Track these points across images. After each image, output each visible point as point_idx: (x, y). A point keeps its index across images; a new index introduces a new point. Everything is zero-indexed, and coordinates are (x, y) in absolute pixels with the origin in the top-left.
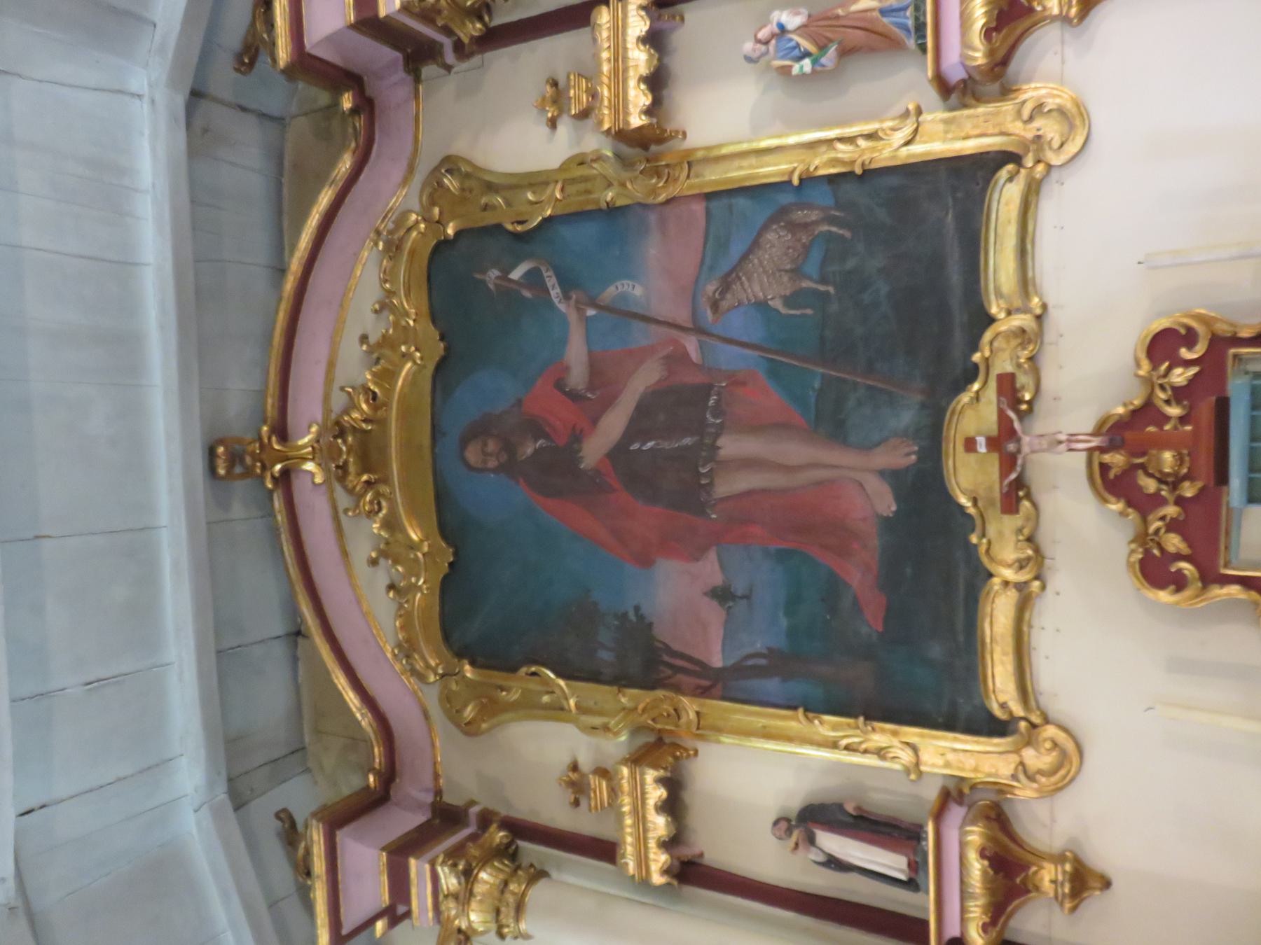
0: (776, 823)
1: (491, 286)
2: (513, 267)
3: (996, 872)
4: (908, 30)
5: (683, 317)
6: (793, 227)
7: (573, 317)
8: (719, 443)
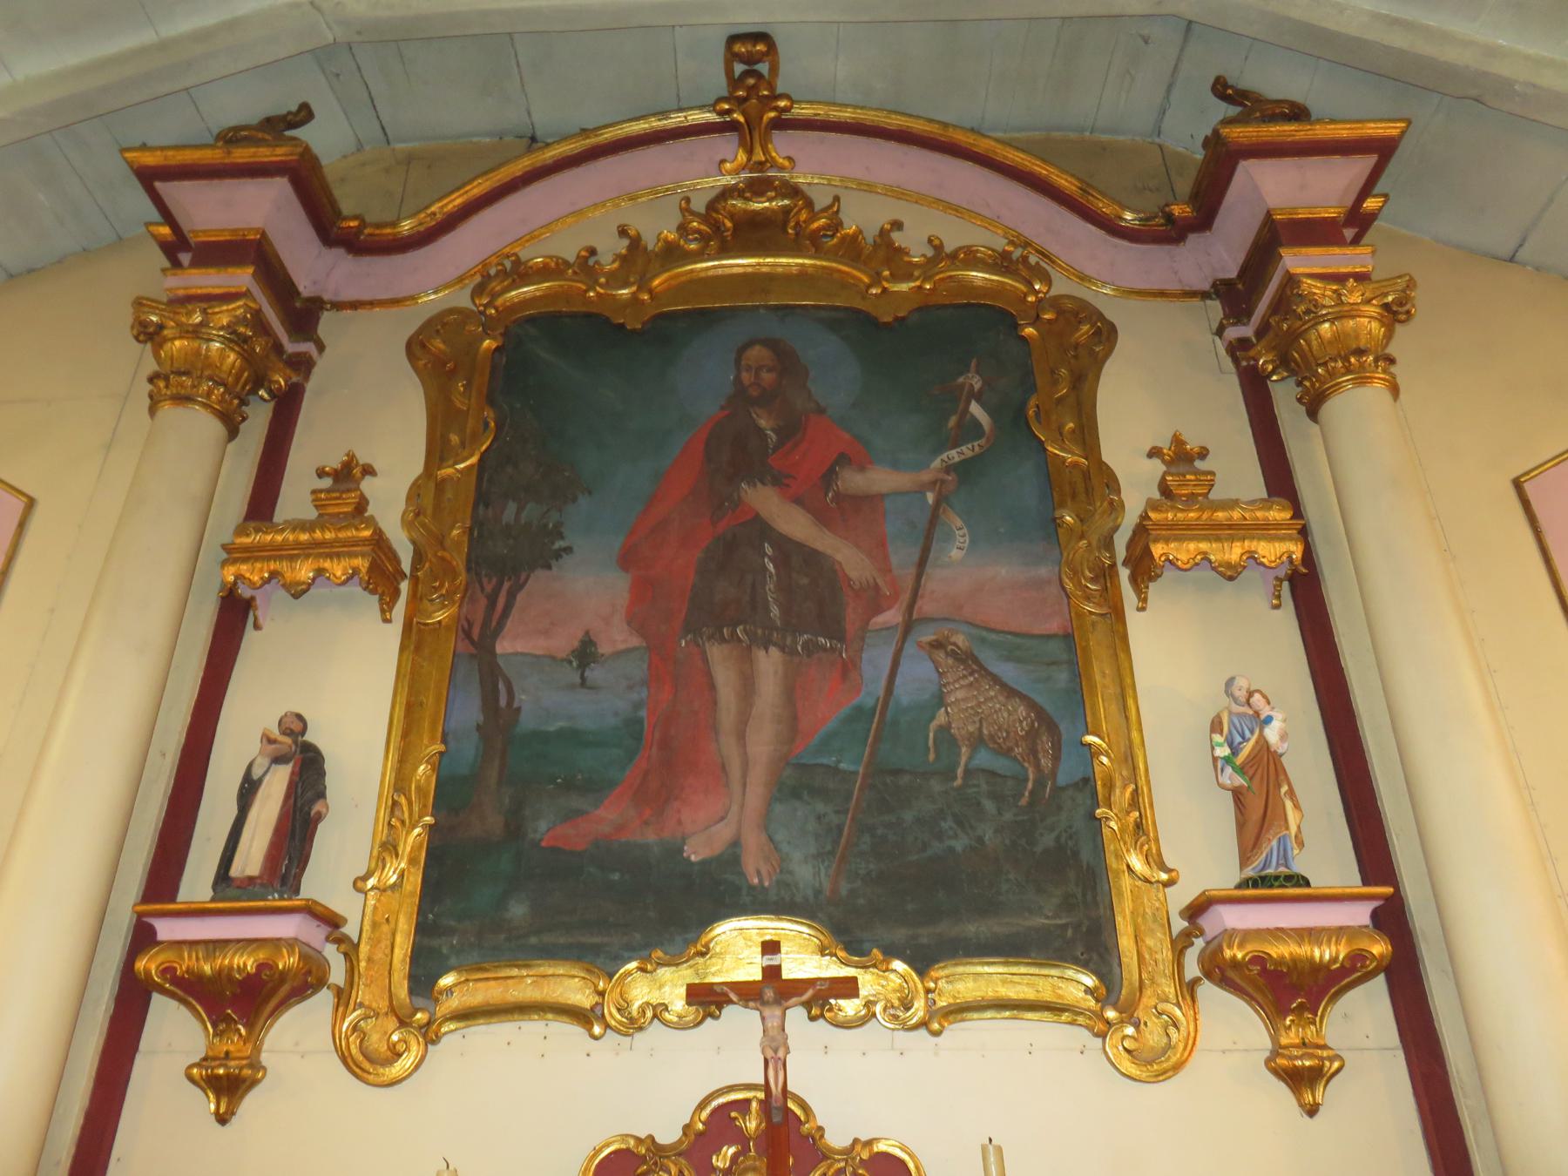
0: (300, 717)
1: (961, 380)
3: (241, 983)
4: (1264, 868)
5: (926, 606)
6: (1032, 735)
7: (926, 476)
8: (773, 651)
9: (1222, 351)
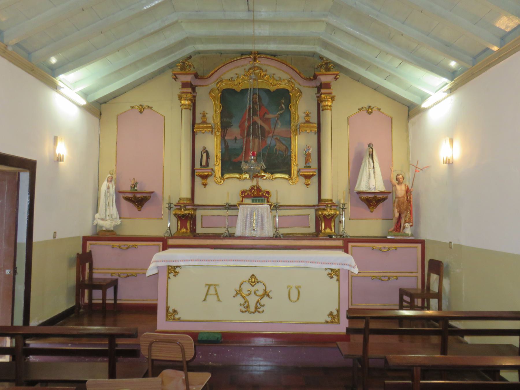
0: (205, 147)
1: (281, 101)
2: (284, 105)
5: (275, 133)
6: (285, 150)
7: (276, 115)
8: (257, 139)
9: (316, 97)
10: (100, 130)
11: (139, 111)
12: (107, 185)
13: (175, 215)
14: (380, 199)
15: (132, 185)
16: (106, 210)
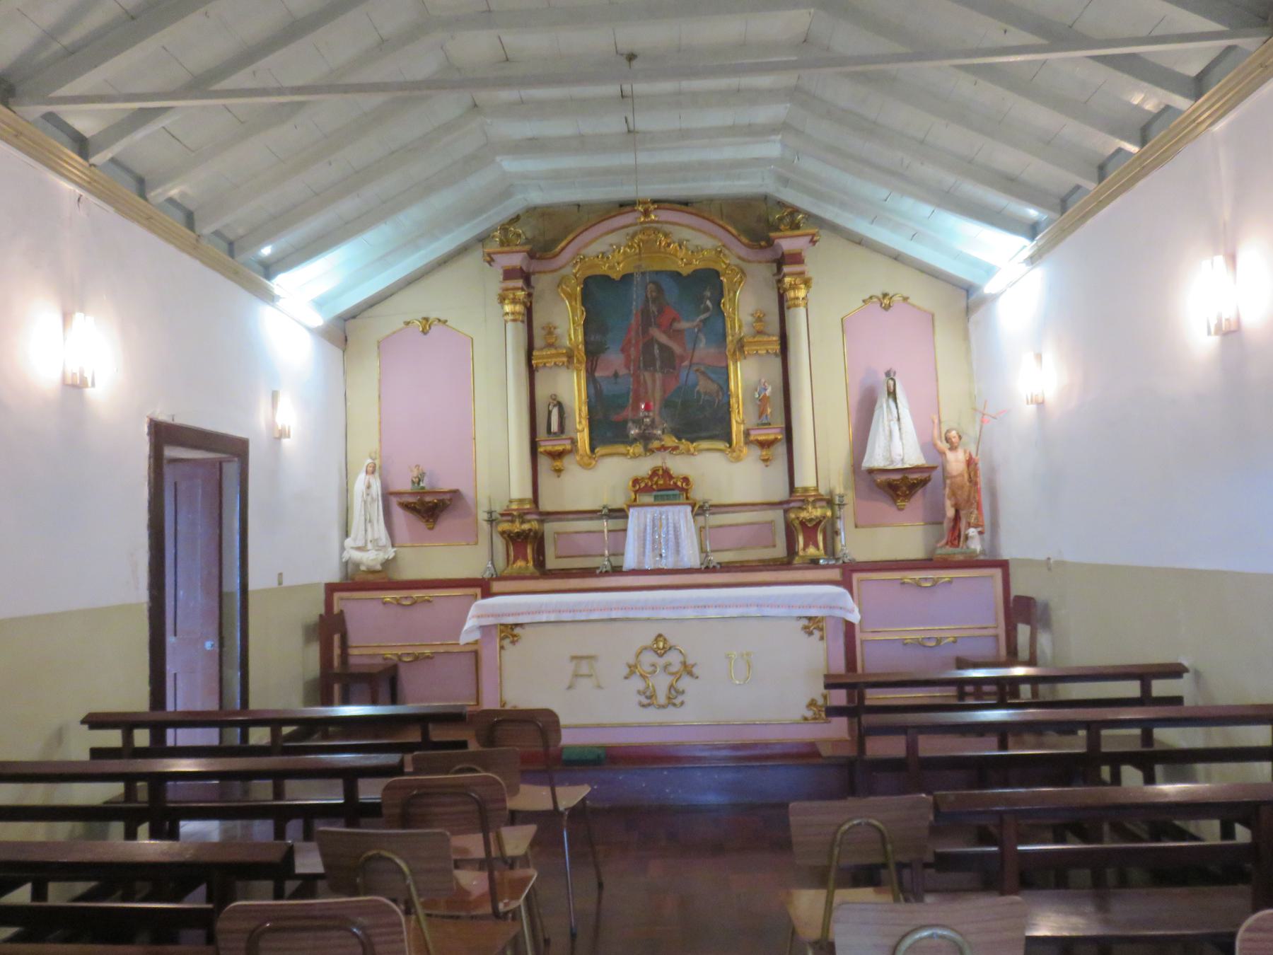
0: (555, 395)
2: (711, 301)
5: (695, 360)
7: (695, 323)
10: (345, 372)
11: (421, 329)
12: (367, 480)
13: (503, 533)
14: (915, 481)
15: (415, 478)
16: (366, 531)
